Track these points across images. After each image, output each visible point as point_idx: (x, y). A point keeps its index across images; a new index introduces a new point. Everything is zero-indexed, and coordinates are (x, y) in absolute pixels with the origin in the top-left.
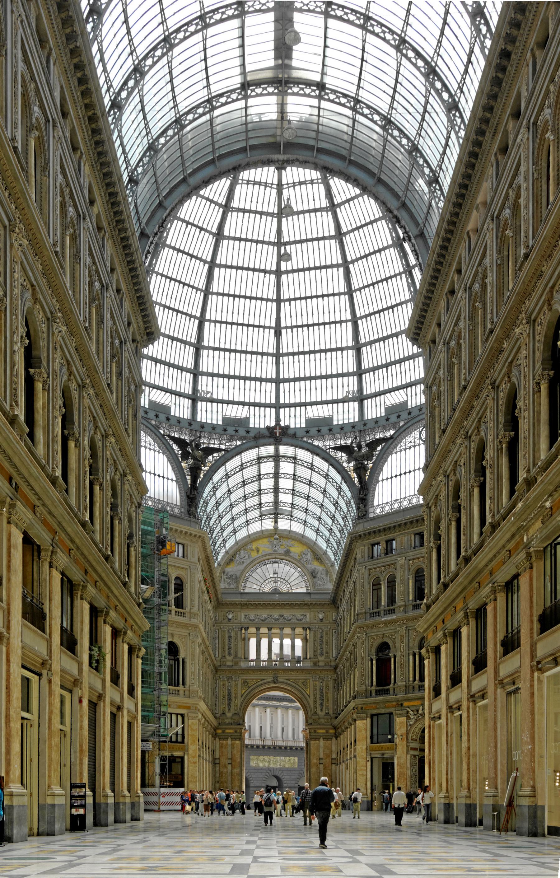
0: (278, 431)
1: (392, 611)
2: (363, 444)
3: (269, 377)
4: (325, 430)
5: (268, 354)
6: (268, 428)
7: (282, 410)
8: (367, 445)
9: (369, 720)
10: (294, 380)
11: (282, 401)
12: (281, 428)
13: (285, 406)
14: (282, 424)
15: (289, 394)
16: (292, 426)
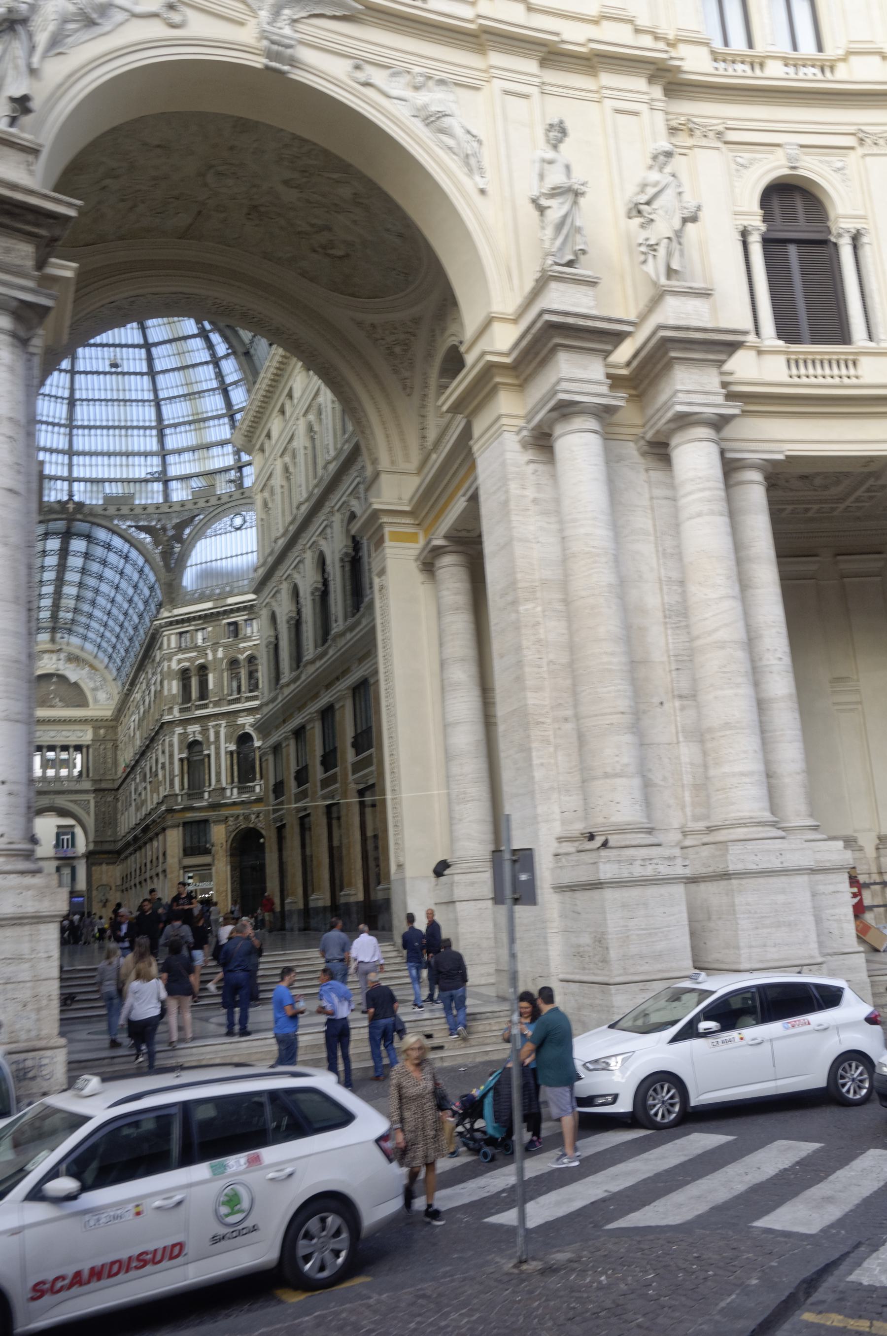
0: (71, 506)
1: (205, 706)
2: (169, 526)
3: (61, 447)
4: (125, 510)
5: (59, 425)
6: (59, 502)
7: (76, 484)
8: (174, 528)
9: (181, 828)
10: (91, 454)
11: (75, 475)
12: (75, 503)
13: (79, 480)
14: (76, 498)
15: (83, 468)
16: (88, 502)
